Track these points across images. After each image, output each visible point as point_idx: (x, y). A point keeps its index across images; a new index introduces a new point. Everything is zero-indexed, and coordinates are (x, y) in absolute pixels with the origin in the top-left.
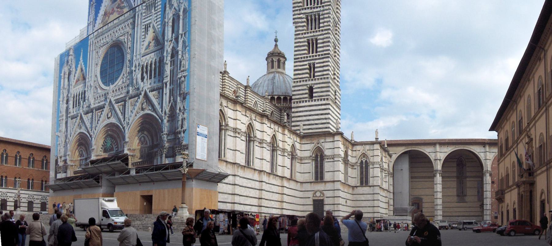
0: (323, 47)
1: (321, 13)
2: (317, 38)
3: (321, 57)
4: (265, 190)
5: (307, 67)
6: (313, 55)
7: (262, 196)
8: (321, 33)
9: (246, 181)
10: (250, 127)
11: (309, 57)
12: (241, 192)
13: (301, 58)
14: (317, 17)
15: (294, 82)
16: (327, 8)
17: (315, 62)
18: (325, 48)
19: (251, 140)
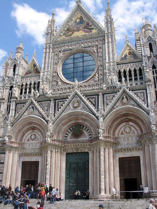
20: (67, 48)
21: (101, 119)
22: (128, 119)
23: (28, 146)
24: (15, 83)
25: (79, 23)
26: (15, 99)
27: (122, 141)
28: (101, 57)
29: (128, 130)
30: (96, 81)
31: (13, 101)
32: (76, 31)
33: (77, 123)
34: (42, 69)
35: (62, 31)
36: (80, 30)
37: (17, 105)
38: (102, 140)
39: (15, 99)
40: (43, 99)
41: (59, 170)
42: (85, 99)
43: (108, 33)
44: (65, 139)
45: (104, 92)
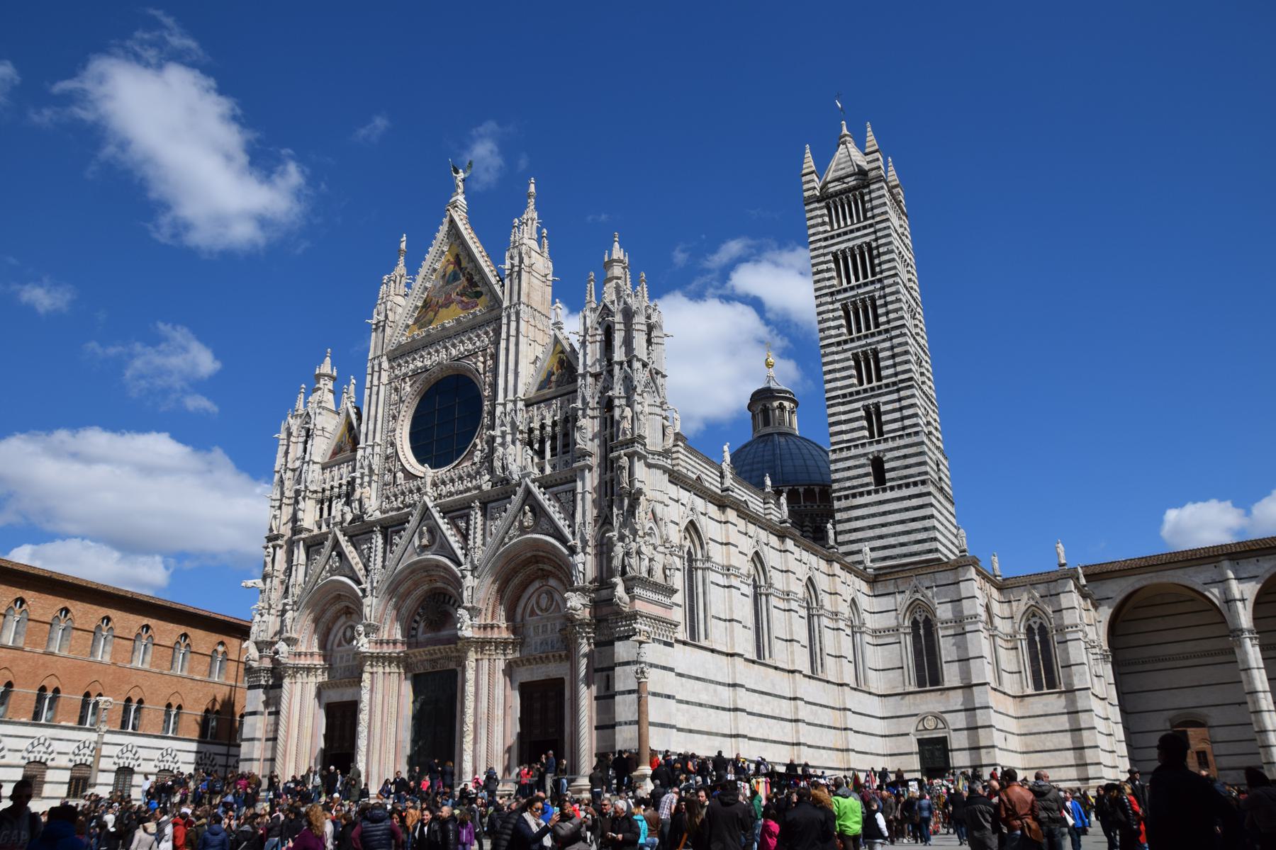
0: (894, 365)
1: (877, 294)
2: (876, 348)
4: (803, 721)
5: (862, 413)
6: (870, 386)
7: (799, 738)
9: (760, 700)
10: (757, 558)
11: (862, 392)
12: (750, 728)
13: (844, 396)
14: (869, 302)
15: (834, 451)
17: (879, 402)
18: (899, 369)
19: (761, 594)
20: (420, 364)
21: (469, 581)
22: (542, 570)
23: (338, 660)
24: (303, 489)
25: (451, 278)
26: (303, 536)
27: (532, 635)
31: (298, 541)
32: (441, 307)
33: (436, 588)
34: (362, 438)
35: (411, 309)
39: (303, 536)
40: (360, 531)
41: (394, 723)
42: (443, 524)
44: (412, 636)
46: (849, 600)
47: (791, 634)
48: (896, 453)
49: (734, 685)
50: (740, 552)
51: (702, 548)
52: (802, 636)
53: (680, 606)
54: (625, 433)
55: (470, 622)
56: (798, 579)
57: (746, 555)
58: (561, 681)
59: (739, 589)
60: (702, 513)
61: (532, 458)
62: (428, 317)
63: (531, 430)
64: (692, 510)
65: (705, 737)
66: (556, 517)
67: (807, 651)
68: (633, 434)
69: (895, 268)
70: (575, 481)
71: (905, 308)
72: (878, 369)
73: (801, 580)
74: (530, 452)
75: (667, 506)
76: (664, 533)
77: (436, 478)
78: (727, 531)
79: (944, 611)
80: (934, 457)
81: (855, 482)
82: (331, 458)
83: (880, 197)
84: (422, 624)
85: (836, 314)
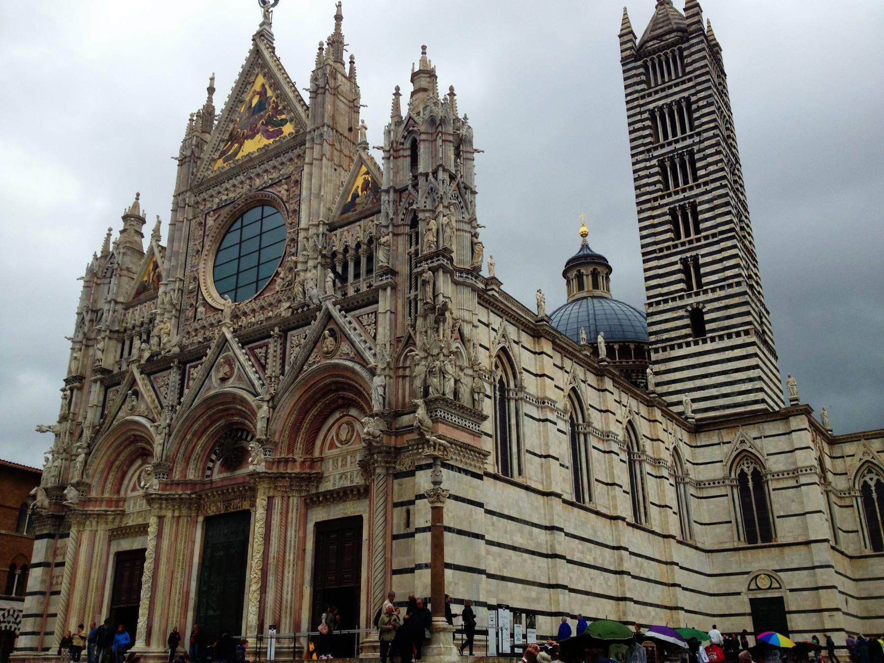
1: (696, 148)
2: (695, 201)
3: (711, 240)
4: (629, 574)
7: (624, 592)
8: (703, 189)
9: (580, 547)
10: (575, 395)
11: (679, 245)
12: (571, 578)
13: (661, 250)
14: (686, 158)
15: (650, 305)
16: (711, 133)
17: (697, 255)
18: (719, 220)
20: (224, 197)
21: (264, 411)
22: (343, 398)
25: (257, 108)
27: (331, 469)
28: (295, 211)
29: (346, 432)
30: (278, 292)
35: (217, 143)
36: (258, 133)
37: (109, 391)
38: (259, 473)
39: (99, 376)
43: (314, 131)
44: (207, 476)
45: (284, 326)
46: (671, 448)
47: (612, 475)
48: (717, 305)
49: (552, 528)
50: (556, 386)
51: (515, 377)
52: (624, 479)
53: (490, 436)
54: (430, 247)
55: (263, 456)
56: (617, 421)
57: (562, 390)
58: (360, 518)
59: (555, 424)
60: (515, 342)
61: (334, 282)
62: (234, 148)
63: (334, 254)
64: (504, 336)
65: (520, 586)
66: (356, 339)
67: (629, 497)
68: (437, 246)
69: (714, 120)
70: (377, 302)
71: (725, 161)
72: (697, 223)
73: (621, 423)
74: (331, 275)
75: (476, 327)
76: (473, 354)
77: (237, 310)
78: (542, 362)
79: (775, 463)
80: (756, 309)
81: (673, 334)
82: (134, 298)
83: (699, 51)
84: (218, 463)
85: (653, 171)
